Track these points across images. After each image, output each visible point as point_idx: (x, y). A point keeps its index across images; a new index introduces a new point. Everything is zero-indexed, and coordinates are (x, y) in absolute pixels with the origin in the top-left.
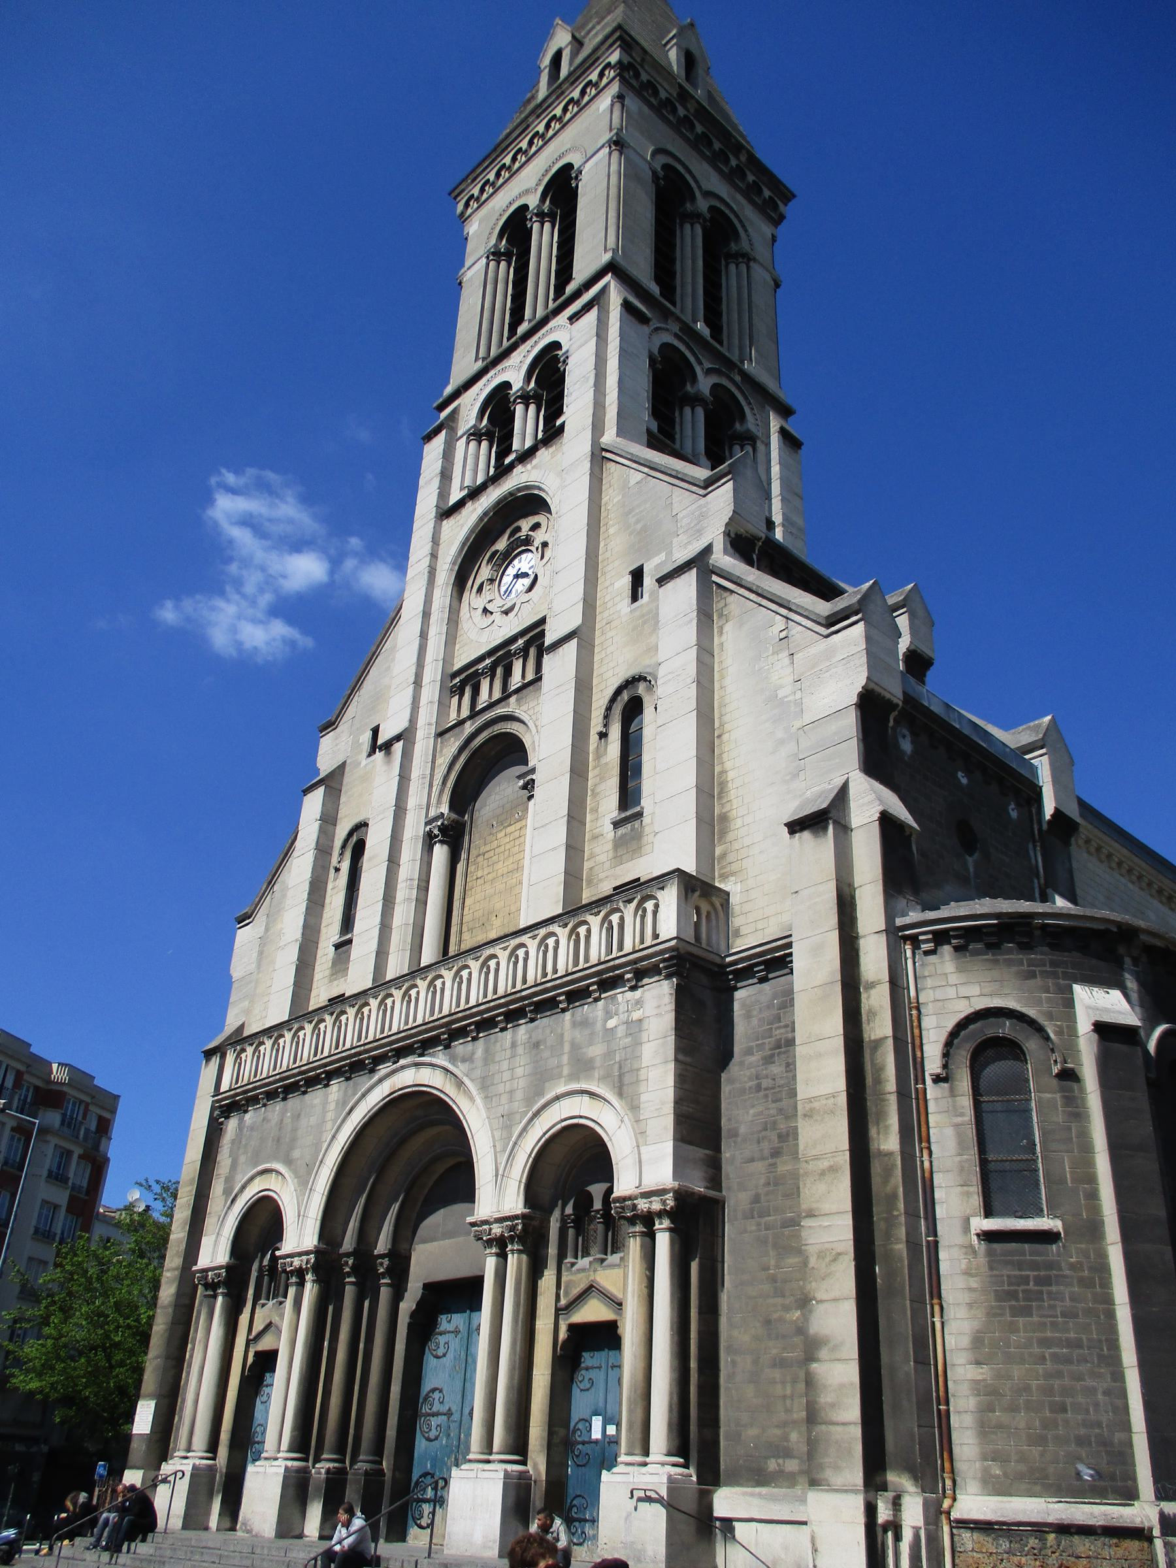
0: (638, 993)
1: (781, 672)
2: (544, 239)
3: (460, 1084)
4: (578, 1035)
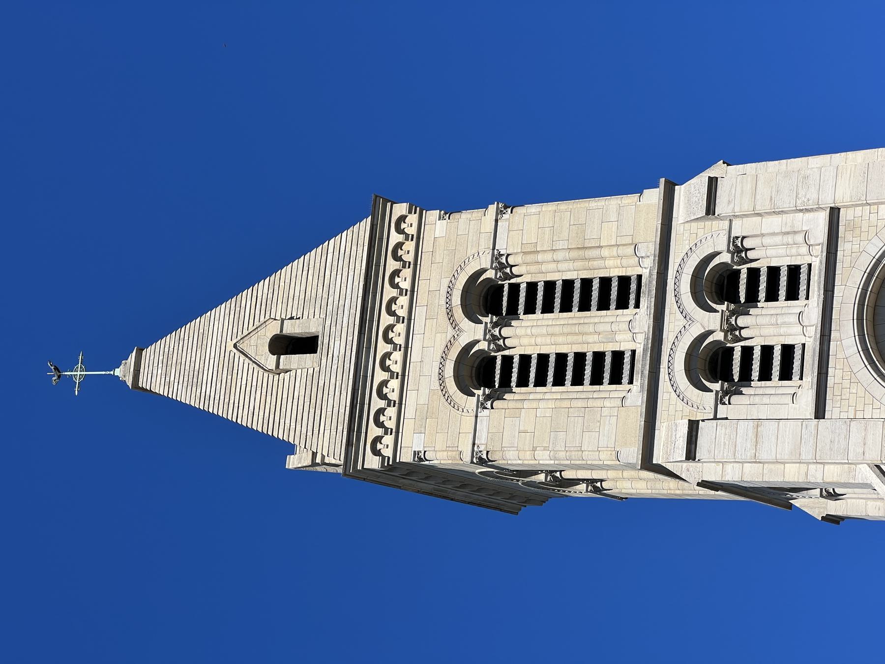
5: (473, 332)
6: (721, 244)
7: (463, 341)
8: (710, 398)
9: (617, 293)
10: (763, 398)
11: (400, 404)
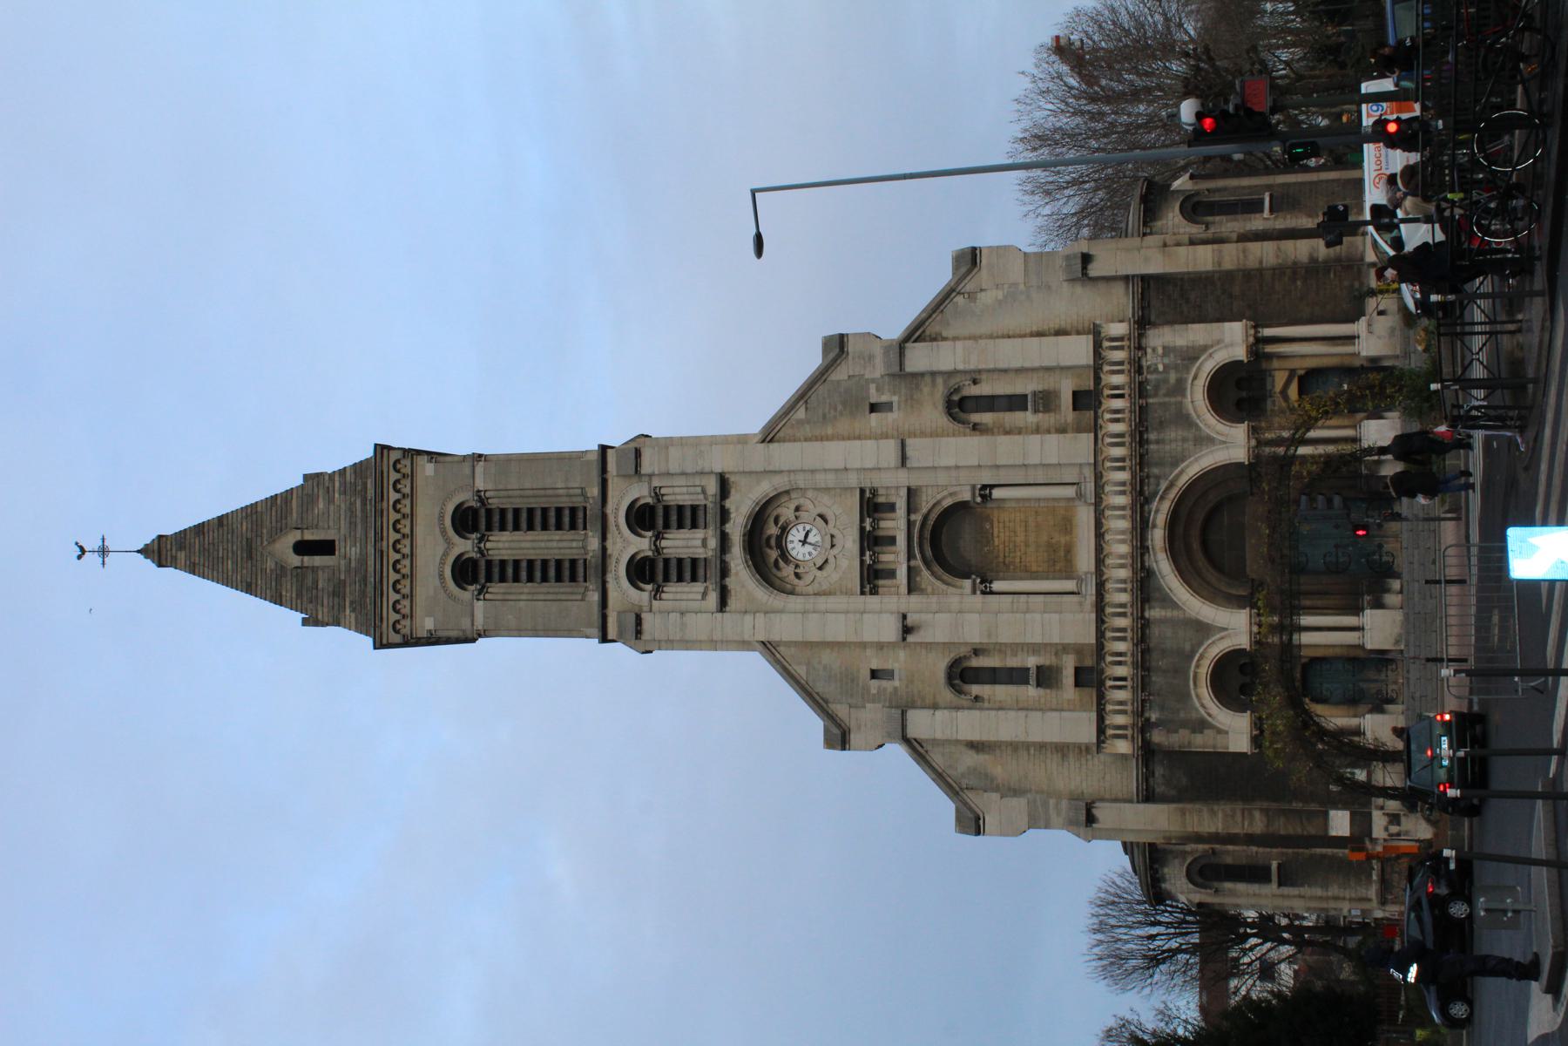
0: (1149, 351)
1: (986, 298)
2: (504, 545)
3: (1171, 485)
4: (1162, 392)
5: (465, 546)
6: (646, 492)
10: (680, 594)
11: (411, 596)
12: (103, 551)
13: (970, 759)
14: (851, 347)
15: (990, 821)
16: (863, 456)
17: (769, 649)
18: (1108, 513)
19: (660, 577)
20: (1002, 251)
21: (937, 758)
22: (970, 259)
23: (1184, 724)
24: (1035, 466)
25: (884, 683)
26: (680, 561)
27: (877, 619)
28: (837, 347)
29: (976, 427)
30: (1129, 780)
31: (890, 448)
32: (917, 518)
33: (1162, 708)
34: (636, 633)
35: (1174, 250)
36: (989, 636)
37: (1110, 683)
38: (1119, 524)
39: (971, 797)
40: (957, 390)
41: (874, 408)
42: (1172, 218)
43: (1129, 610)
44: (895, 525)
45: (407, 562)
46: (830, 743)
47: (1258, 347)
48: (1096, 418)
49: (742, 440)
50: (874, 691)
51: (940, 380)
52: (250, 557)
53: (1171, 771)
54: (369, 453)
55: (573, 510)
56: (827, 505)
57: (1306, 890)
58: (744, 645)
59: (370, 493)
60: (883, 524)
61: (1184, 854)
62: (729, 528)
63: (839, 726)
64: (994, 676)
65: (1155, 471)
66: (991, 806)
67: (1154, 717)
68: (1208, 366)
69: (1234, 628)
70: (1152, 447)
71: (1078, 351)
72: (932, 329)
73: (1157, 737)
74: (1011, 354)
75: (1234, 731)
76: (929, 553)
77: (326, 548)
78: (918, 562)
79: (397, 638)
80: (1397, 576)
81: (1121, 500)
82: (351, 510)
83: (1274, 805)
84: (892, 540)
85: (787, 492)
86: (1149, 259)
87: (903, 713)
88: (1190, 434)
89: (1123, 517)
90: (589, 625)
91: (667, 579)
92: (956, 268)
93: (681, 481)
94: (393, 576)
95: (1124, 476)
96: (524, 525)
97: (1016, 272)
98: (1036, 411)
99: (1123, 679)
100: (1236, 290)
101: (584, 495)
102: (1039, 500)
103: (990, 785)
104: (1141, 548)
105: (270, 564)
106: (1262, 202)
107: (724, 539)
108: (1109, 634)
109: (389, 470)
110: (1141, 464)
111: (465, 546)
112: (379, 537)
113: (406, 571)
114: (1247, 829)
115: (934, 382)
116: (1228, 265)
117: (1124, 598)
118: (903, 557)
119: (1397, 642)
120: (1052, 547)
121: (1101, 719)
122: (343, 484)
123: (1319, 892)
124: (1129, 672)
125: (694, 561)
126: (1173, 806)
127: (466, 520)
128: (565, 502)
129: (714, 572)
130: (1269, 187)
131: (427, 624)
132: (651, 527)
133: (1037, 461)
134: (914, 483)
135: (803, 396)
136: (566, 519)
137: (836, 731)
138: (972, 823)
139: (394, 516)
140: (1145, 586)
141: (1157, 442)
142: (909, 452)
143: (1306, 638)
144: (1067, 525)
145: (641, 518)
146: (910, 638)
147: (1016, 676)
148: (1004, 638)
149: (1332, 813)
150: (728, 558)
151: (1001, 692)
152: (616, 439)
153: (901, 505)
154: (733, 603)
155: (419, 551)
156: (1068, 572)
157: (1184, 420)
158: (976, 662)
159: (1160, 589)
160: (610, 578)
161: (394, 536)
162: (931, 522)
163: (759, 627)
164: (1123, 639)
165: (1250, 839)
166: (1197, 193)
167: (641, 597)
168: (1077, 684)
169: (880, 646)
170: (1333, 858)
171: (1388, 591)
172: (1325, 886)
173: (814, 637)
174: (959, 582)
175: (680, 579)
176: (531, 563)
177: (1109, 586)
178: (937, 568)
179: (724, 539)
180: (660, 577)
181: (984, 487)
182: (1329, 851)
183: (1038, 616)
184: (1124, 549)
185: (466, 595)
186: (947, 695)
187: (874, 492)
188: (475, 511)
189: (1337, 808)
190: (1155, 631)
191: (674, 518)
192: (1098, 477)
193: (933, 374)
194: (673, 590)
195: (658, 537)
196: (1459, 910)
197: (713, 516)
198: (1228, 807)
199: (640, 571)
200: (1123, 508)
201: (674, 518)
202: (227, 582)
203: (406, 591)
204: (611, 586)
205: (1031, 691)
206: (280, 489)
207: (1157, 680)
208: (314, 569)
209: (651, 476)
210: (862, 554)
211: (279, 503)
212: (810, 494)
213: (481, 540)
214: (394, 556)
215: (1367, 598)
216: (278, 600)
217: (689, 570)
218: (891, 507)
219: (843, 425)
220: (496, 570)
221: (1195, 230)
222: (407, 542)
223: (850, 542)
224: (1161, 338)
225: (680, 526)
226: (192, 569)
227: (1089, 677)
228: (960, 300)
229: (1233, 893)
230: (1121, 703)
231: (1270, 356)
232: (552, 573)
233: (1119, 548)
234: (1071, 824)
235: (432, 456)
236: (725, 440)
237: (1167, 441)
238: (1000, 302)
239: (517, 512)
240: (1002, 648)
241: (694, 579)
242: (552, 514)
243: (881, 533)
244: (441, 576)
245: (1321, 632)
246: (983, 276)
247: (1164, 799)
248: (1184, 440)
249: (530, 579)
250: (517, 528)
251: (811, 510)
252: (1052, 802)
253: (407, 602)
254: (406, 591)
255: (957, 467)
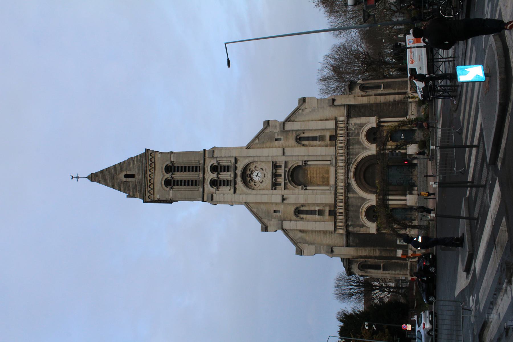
1: (307, 111)
2: (178, 176)
4: (354, 135)
5: (168, 176)
6: (215, 162)
7: (165, 177)
8: (214, 189)
9: (195, 169)
10: (224, 189)
12: (78, 177)
13: (300, 235)
14: (271, 124)
15: (305, 252)
16: (273, 152)
17: (247, 204)
18: (338, 168)
19: (219, 185)
20: (311, 98)
21: (291, 234)
22: (303, 100)
23: (358, 225)
24: (319, 155)
25: (277, 214)
26: (224, 181)
27: (276, 196)
28: (267, 123)
29: (303, 145)
30: (342, 241)
31: (280, 150)
32: (287, 169)
33: (352, 221)
34: (211, 200)
35: (358, 98)
36: (306, 201)
37: (338, 214)
38: (341, 171)
39: (300, 245)
40: (299, 135)
41: (276, 140)
42: (357, 90)
43: (343, 194)
44: (281, 171)
45: (153, 180)
46: (262, 230)
47: (379, 123)
48: (336, 142)
49: (241, 148)
50: (274, 216)
51: (294, 132)
52: (113, 179)
53: (354, 238)
54: (144, 151)
55: (196, 167)
56: (263, 166)
57: (390, 272)
58: (240, 203)
59: (144, 162)
60: (278, 171)
61: (357, 262)
62: (237, 171)
63: (265, 225)
64: (307, 212)
65: (351, 157)
66: (306, 248)
67: (350, 223)
68: (366, 128)
69: (372, 199)
70: (351, 150)
71: (331, 125)
72: (292, 119)
73: (351, 229)
74: (313, 125)
75: (372, 228)
76: (290, 179)
77: (132, 176)
78: (287, 181)
79: (149, 200)
80: (416, 186)
81: (342, 164)
82: (139, 166)
83: (382, 248)
84: (280, 176)
85: (253, 162)
86: (351, 100)
87: (282, 222)
88: (361, 147)
89: (342, 169)
90: (200, 197)
91: (220, 185)
92: (299, 103)
93: (225, 159)
94: (149, 184)
95: (343, 158)
96: (183, 170)
97: (315, 104)
98: (320, 141)
99: (342, 213)
100: (374, 109)
101: (199, 163)
102: (320, 165)
103: (305, 242)
104: (347, 177)
105: (118, 181)
106: (381, 86)
107: (236, 175)
108: (338, 201)
109: (149, 156)
110: (348, 155)
111: (168, 176)
112: (146, 173)
113: (152, 182)
114: (375, 255)
115: (292, 134)
116: (372, 102)
117: (342, 191)
118: (283, 180)
119: (416, 204)
120: (323, 178)
121: (335, 224)
122: (137, 159)
123: (394, 272)
124: (344, 211)
125: (228, 181)
126: (354, 248)
127: (169, 169)
128: (194, 165)
129: (233, 183)
130: (383, 83)
131: (157, 197)
132: (217, 171)
133: (319, 154)
134: (286, 160)
135: (258, 137)
136: (195, 169)
137: (264, 227)
138: (300, 252)
139: (150, 168)
140: (348, 188)
141: (352, 149)
142: (285, 151)
143: (391, 202)
144: (328, 172)
145: (214, 169)
146: (285, 202)
147: (313, 212)
148: (310, 201)
149: (398, 250)
150: (236, 179)
151: (309, 216)
152: (208, 148)
153: (283, 166)
154: (237, 192)
155: (156, 177)
156: (327, 184)
157: (359, 143)
158: (302, 209)
159: (352, 188)
160: (205, 185)
161: (149, 173)
162: (291, 170)
163: (245, 198)
164: (342, 202)
165: (375, 257)
166: (364, 84)
167: (213, 190)
168: (329, 215)
169: (277, 204)
170: (398, 263)
171: (414, 190)
172: (395, 271)
173: (259, 201)
174: (298, 187)
175: (224, 185)
176: (185, 181)
177: (338, 188)
178: (292, 183)
179: (236, 175)
180: (219, 185)
181: (305, 161)
182: (397, 261)
183: (319, 196)
184: (342, 178)
185: (168, 189)
186: (294, 217)
187: (276, 162)
188: (171, 167)
189: (399, 249)
190: (351, 200)
191: (223, 169)
192: (336, 158)
193: (292, 131)
194: (222, 188)
195: (218, 174)
196: (432, 269)
197: (233, 168)
198: (369, 249)
199: (214, 183)
200: (342, 167)
201: (223, 169)
202: (108, 185)
203: (152, 187)
204: (205, 187)
205: (317, 217)
206: (121, 161)
207: (351, 213)
208: (129, 182)
209: (217, 157)
210: (272, 179)
211: (121, 165)
212: (259, 163)
213: (172, 174)
214: (149, 178)
215: (408, 192)
216: (120, 190)
217: (226, 183)
218: (280, 167)
219: (268, 144)
220: (176, 183)
221: (363, 93)
222: (153, 175)
223: (269, 176)
224: (354, 121)
225: (224, 171)
226: (99, 183)
227: (333, 213)
228: (300, 111)
229: (370, 272)
230: (341, 220)
231: (383, 126)
232: (190, 183)
233: (341, 177)
234: (327, 253)
235: (160, 153)
236: (237, 148)
237: (354, 149)
238: (310, 112)
239: (182, 167)
240: (309, 205)
241: (228, 185)
242: (191, 168)
243: (277, 173)
244: (161, 184)
245: (395, 201)
246: (306, 105)
247: (352, 246)
248: (359, 148)
249: (185, 185)
250: (181, 171)
251: (259, 167)
252: (322, 247)
253: (152, 191)
254: (152, 187)
255: (298, 156)
